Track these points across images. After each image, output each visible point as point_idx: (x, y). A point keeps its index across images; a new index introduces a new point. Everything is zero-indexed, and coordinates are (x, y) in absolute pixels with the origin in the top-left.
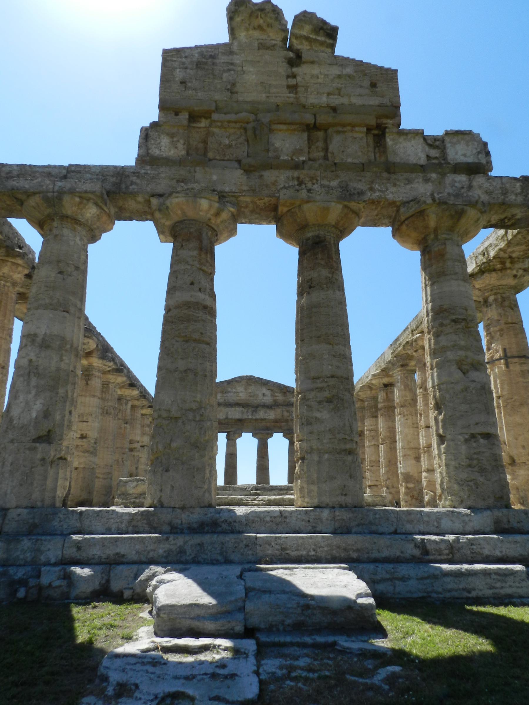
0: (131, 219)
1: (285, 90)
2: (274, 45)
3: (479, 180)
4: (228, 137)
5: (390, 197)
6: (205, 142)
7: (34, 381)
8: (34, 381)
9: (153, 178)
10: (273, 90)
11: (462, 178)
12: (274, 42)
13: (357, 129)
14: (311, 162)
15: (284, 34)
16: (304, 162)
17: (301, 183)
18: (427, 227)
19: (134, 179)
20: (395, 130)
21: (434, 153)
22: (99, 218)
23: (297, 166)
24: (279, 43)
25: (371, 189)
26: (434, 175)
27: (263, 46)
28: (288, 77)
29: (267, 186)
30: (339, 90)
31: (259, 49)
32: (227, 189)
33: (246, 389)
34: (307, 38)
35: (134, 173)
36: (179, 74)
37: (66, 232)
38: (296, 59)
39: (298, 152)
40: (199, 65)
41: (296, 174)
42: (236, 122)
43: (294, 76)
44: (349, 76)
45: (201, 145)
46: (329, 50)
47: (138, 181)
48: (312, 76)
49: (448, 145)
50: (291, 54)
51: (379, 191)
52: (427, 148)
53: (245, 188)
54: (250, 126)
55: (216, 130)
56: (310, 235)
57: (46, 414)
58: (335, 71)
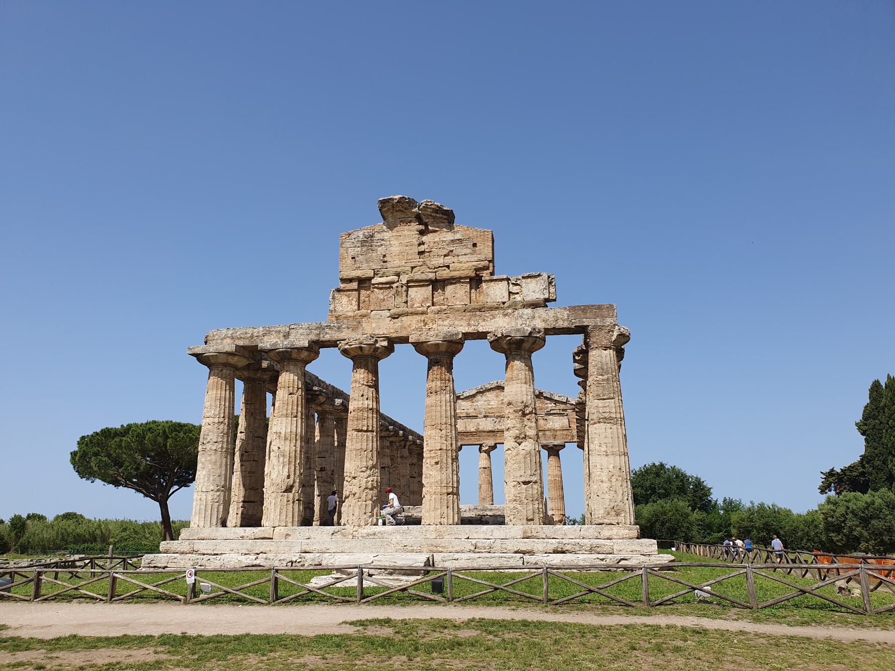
3: (541, 311)
5: (481, 329)
7: (281, 459)
8: (281, 459)
11: (529, 311)
18: (503, 348)
19: (327, 330)
21: (515, 289)
23: (423, 313)
25: (469, 325)
26: (510, 311)
28: (419, 245)
30: (452, 251)
33: (497, 396)
36: (352, 252)
40: (363, 243)
41: (423, 317)
42: (386, 283)
49: (523, 285)
50: (422, 227)
52: (511, 285)
53: (392, 331)
54: (394, 285)
57: (289, 477)
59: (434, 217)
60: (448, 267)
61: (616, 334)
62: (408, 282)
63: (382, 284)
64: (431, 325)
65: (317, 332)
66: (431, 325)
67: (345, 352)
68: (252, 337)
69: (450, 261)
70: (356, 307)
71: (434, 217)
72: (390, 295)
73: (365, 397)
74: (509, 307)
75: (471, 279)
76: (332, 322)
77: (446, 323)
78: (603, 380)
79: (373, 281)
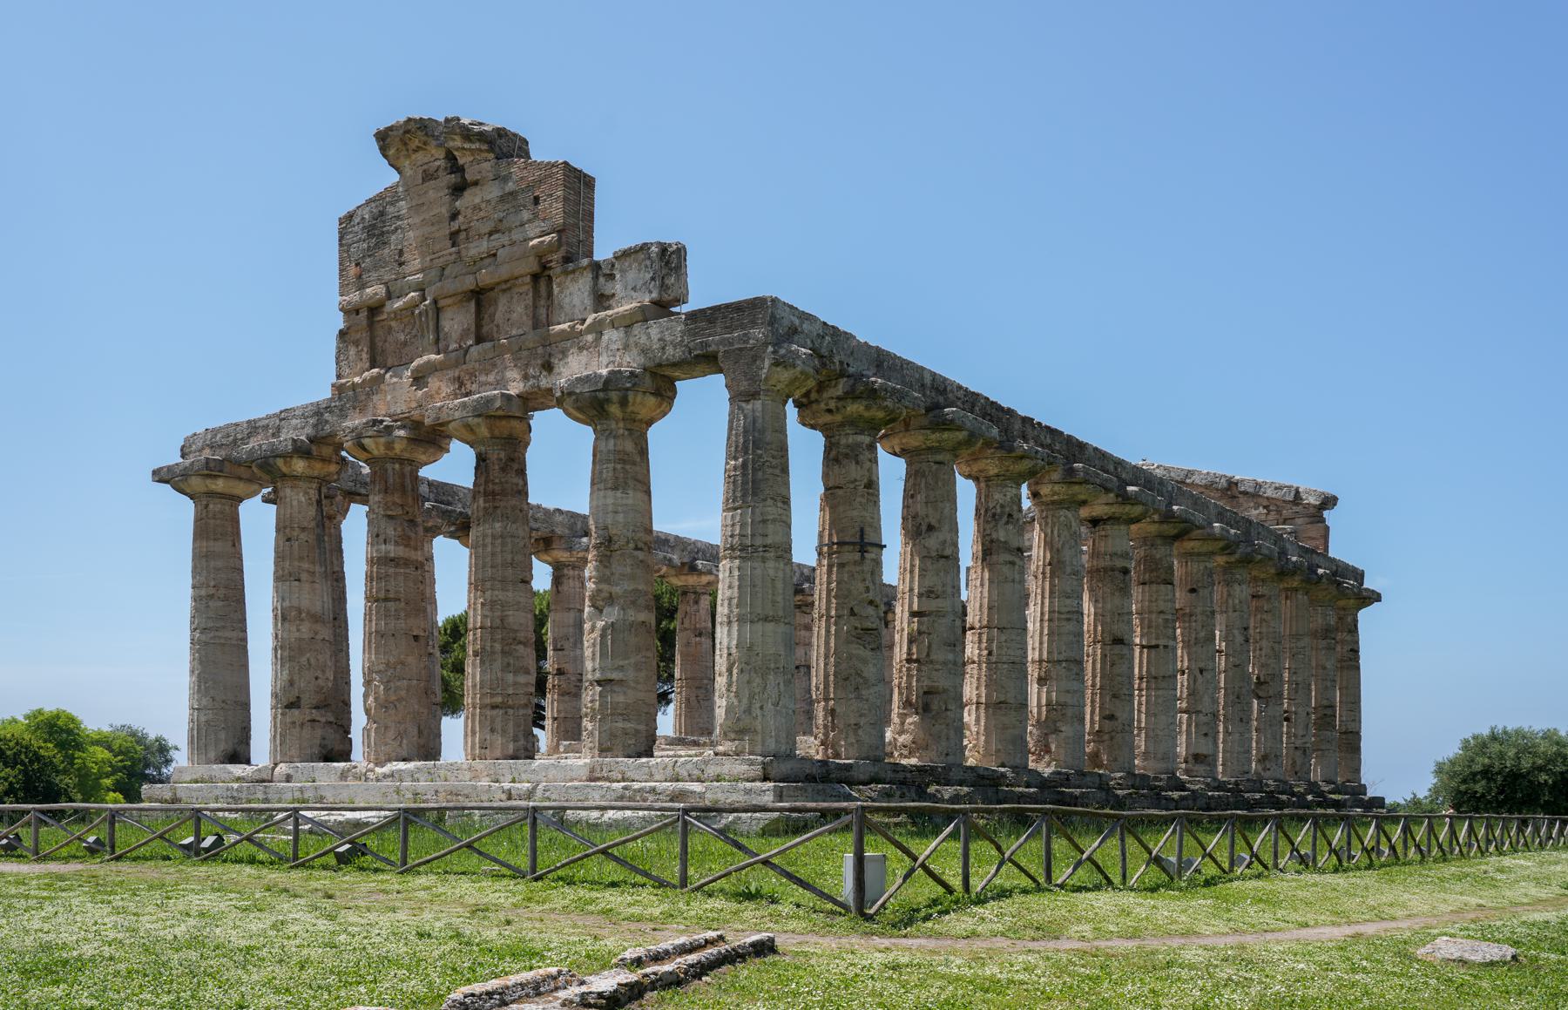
26: (590, 338)
39: (464, 335)
74: (589, 330)
77: (491, 378)
78: (735, 468)
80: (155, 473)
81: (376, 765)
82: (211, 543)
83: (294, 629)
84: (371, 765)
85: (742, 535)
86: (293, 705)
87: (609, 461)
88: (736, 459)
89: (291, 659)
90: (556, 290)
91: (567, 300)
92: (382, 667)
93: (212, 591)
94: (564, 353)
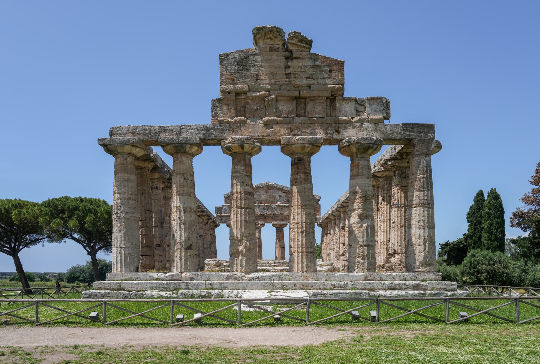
0: (210, 145)
1: (285, 77)
2: (278, 49)
4: (256, 105)
6: (244, 107)
9: (221, 130)
10: (279, 77)
12: (279, 46)
13: (321, 98)
14: (297, 118)
15: (283, 42)
16: (293, 118)
17: (292, 131)
20: (340, 98)
22: (197, 150)
23: (289, 123)
24: (281, 47)
25: (326, 133)
27: (272, 50)
29: (275, 133)
31: (270, 51)
32: (256, 135)
34: (296, 44)
35: (212, 128)
37: (184, 159)
38: (290, 57)
43: (289, 67)
44: (318, 66)
45: (242, 109)
46: (308, 50)
47: (214, 132)
48: (299, 67)
51: (330, 134)
52: (357, 105)
53: (265, 134)
55: (250, 101)
56: (297, 156)
58: (309, 63)
59: (298, 46)
60: (310, 87)
61: (433, 145)
62: (277, 97)
63: (256, 97)
64: (296, 132)
65: (204, 132)
66: (296, 132)
67: (227, 150)
68: (150, 133)
69: (311, 83)
70: (234, 115)
71: (298, 46)
72: (262, 106)
73: (245, 184)
75: (327, 98)
76: (216, 125)
78: (423, 178)
79: (249, 94)
80: (99, 140)
81: (246, 274)
82: (129, 175)
83: (189, 216)
84: (243, 274)
85: (427, 200)
86: (189, 248)
87: (366, 169)
88: (423, 174)
89: (189, 229)
90: (338, 105)
91: (343, 109)
92: (247, 235)
93: (130, 196)
94: (346, 128)
